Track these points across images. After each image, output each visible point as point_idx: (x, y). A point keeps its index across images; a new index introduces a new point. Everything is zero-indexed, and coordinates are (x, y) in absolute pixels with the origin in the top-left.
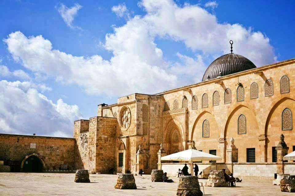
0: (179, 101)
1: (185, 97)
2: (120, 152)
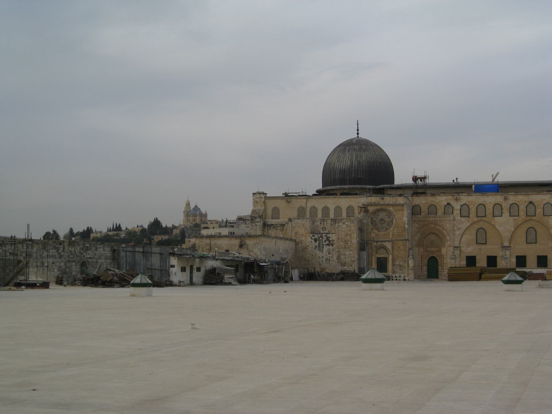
0: (437, 207)
1: (449, 204)
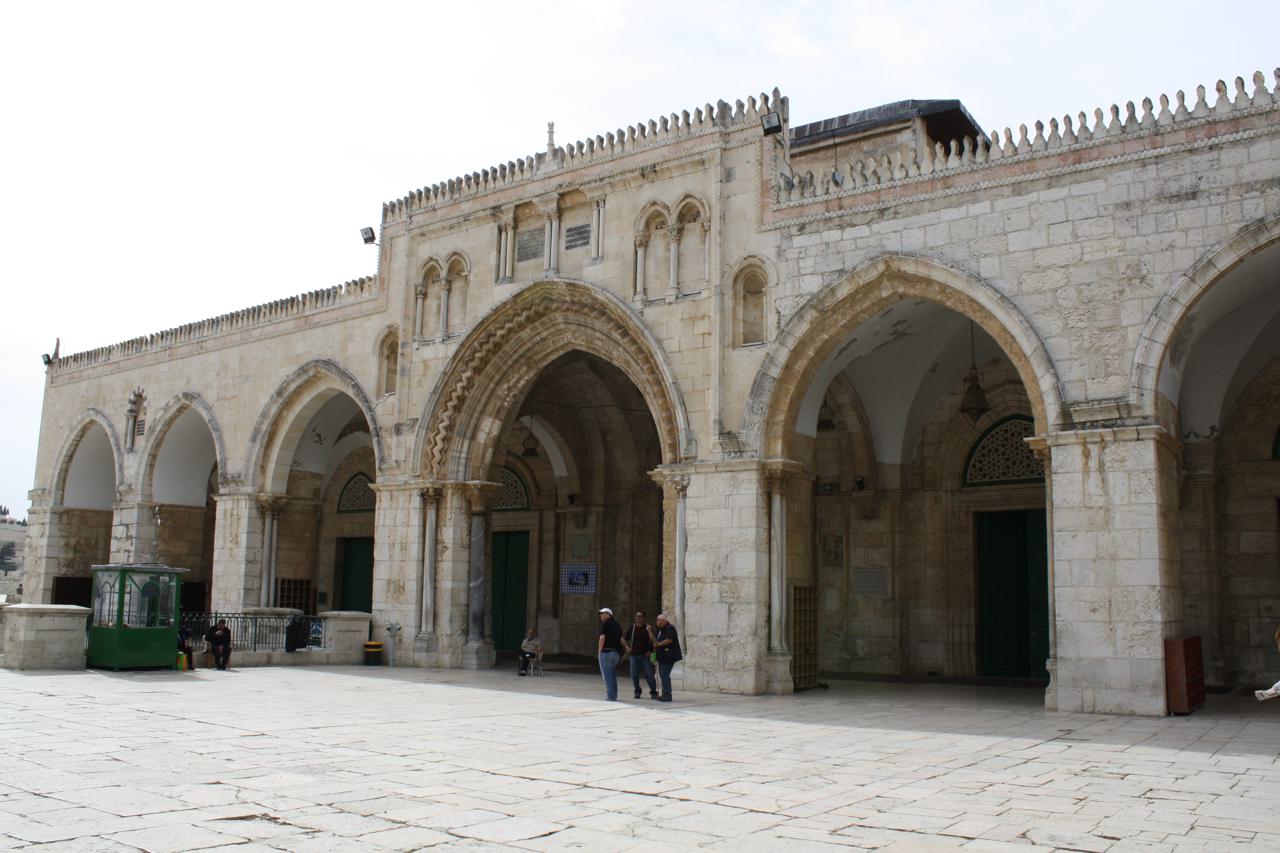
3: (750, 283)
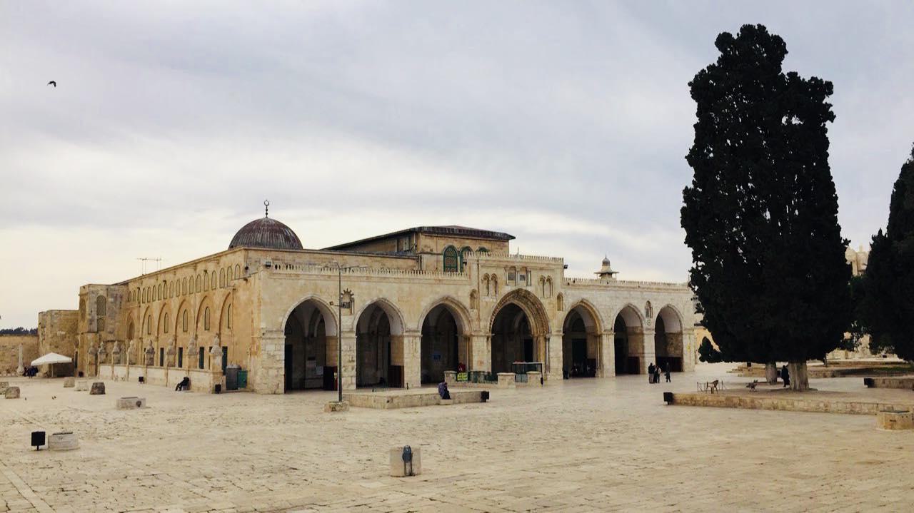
1: (139, 288)
2: (76, 350)
3: (560, 297)
